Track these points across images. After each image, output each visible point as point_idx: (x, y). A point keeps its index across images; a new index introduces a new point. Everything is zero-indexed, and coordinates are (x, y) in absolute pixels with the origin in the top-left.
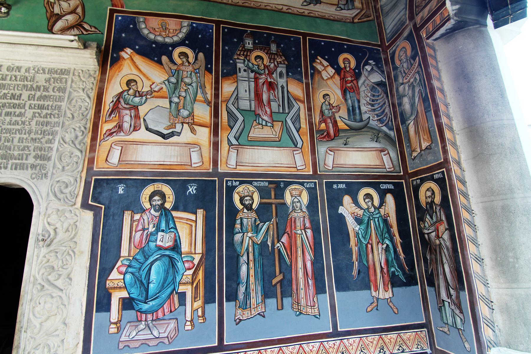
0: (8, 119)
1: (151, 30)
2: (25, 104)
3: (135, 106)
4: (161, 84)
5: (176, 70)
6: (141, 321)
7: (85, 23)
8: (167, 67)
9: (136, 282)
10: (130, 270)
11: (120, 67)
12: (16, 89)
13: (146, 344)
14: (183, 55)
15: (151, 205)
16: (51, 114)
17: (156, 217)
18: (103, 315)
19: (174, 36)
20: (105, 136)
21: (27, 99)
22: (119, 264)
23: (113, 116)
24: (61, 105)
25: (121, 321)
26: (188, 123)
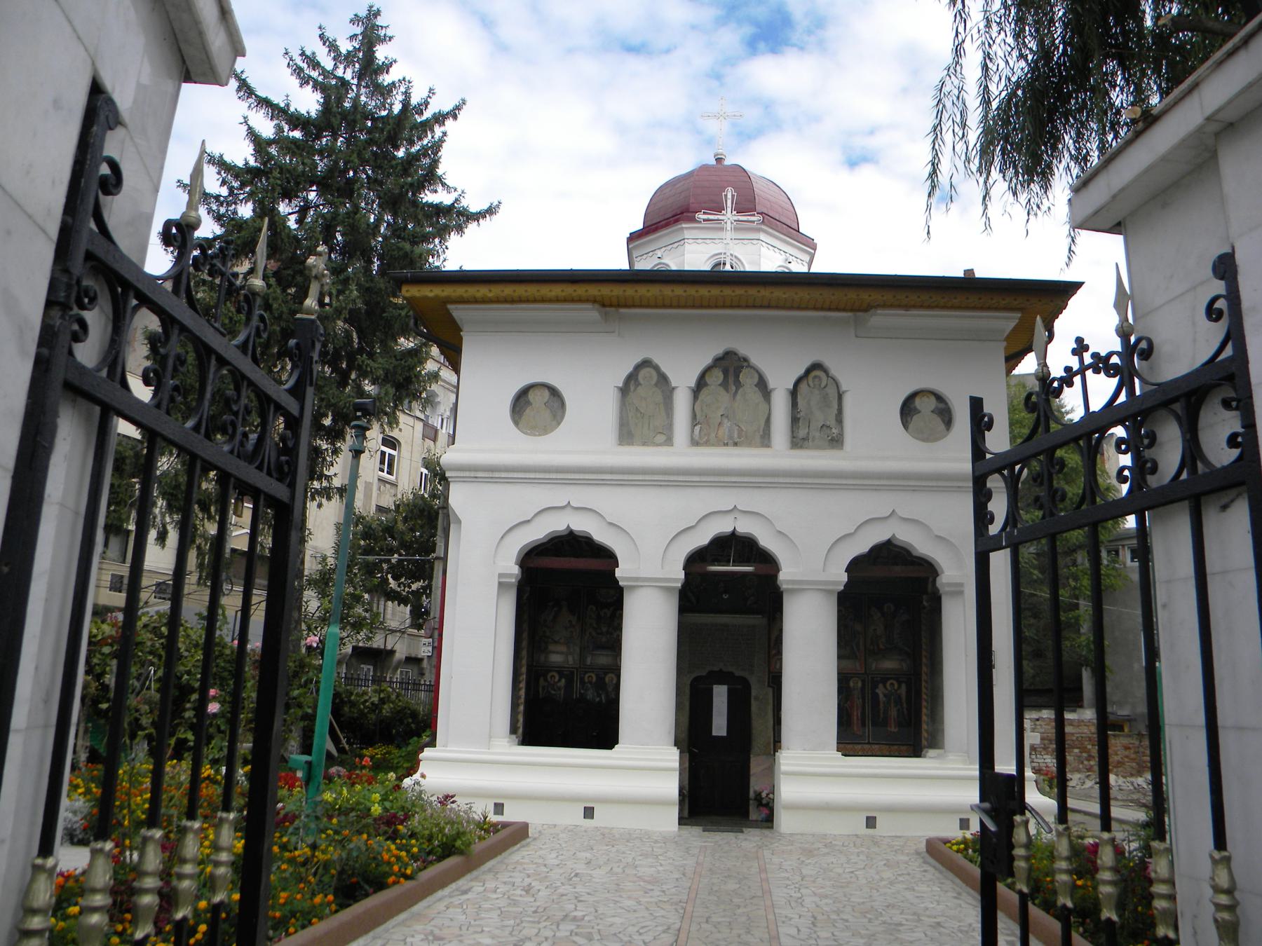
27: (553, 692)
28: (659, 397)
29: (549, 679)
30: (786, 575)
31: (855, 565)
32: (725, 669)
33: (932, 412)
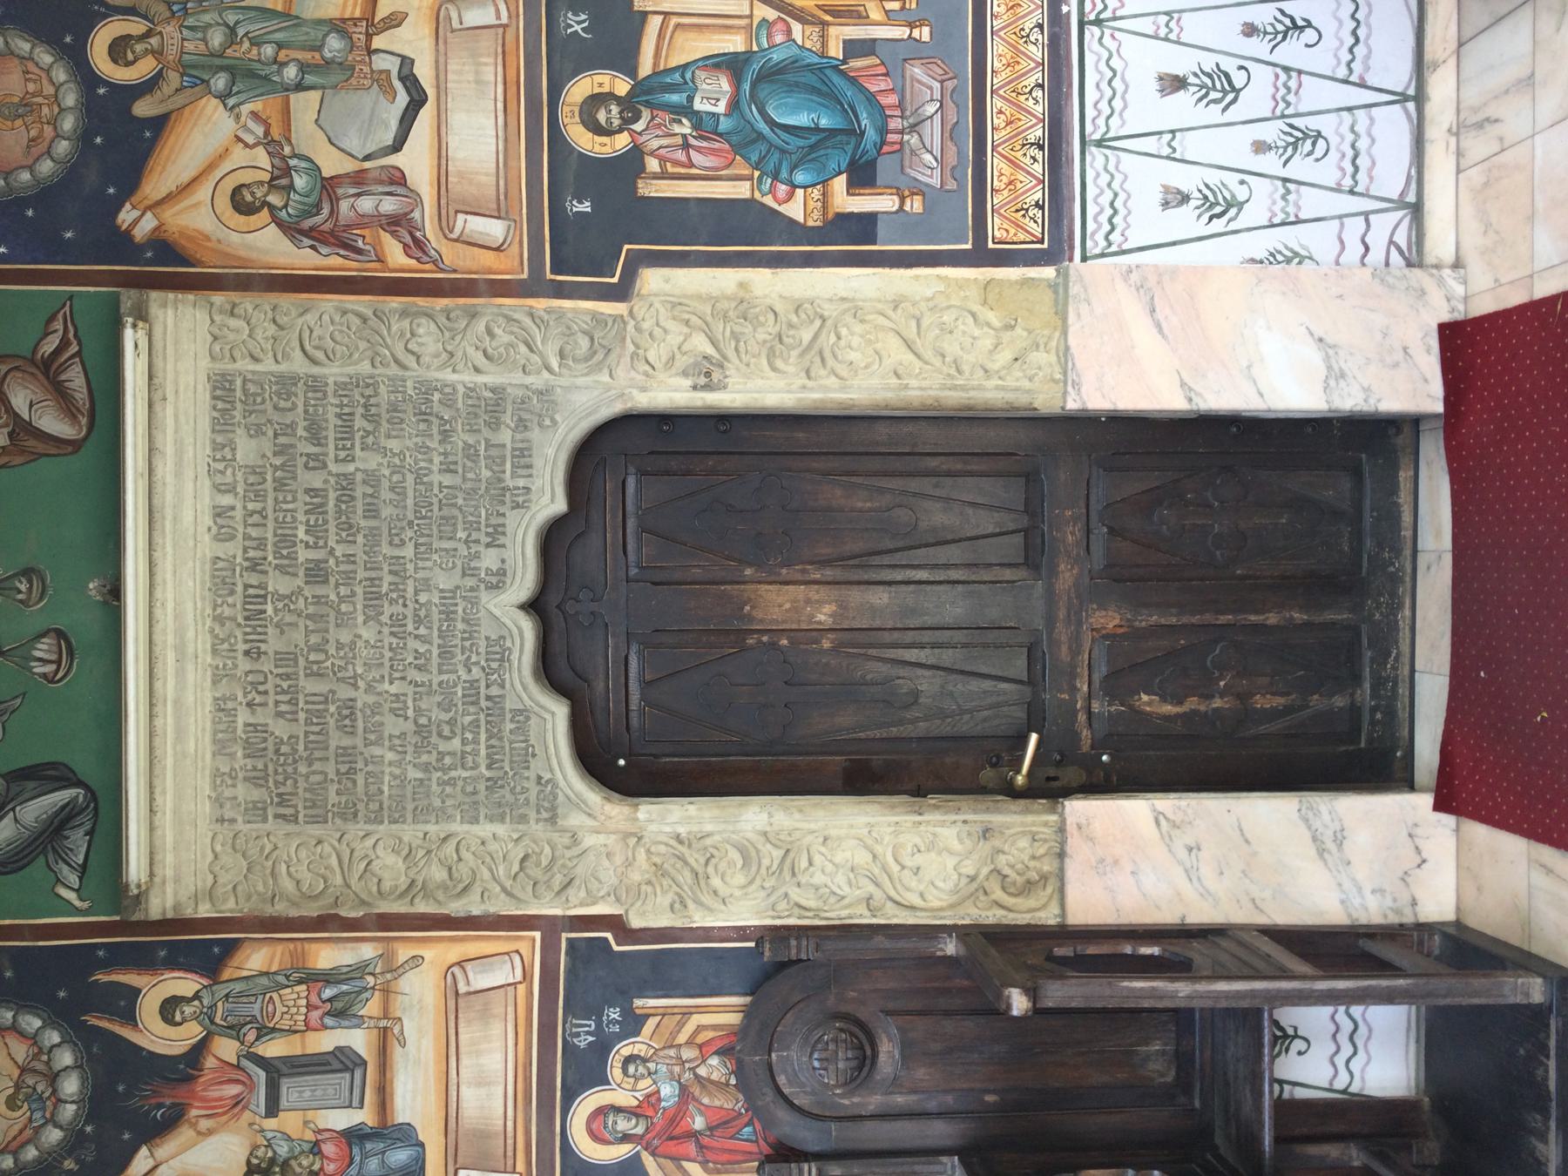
0: (386, 512)
1: (35, 151)
2: (338, 475)
3: (323, 187)
4: (238, 117)
5: (182, 75)
6: (901, 143)
7: (35, 351)
8: (175, 98)
9: (813, 160)
10: (784, 174)
11: (190, 238)
12: (290, 506)
13: (952, 130)
14: (118, 50)
15: (620, 131)
16: (365, 406)
17: (653, 118)
18: (882, 229)
19: (51, 81)
20: (426, 259)
21: (321, 475)
22: (768, 201)
23: (360, 244)
24: (335, 383)
25: (898, 189)
26: (369, 37)
32: (525, 582)
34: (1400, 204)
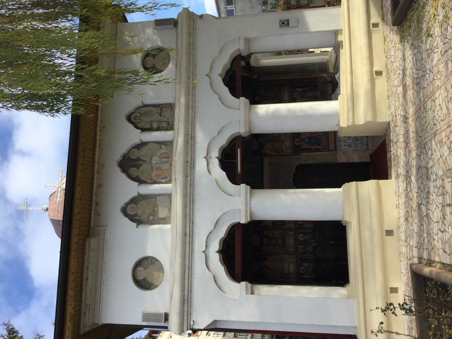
14: (262, 140)
27: (311, 270)
28: (143, 202)
29: (303, 272)
30: (243, 130)
31: (235, 93)
32: (292, 178)
33: (154, 59)
34: (366, 145)
